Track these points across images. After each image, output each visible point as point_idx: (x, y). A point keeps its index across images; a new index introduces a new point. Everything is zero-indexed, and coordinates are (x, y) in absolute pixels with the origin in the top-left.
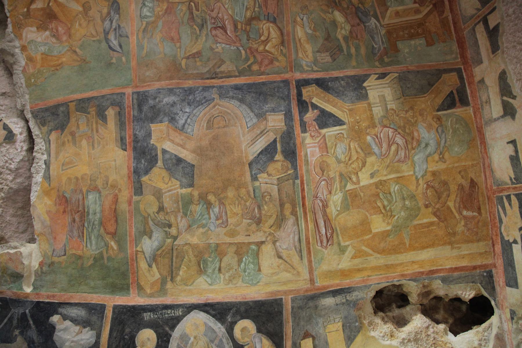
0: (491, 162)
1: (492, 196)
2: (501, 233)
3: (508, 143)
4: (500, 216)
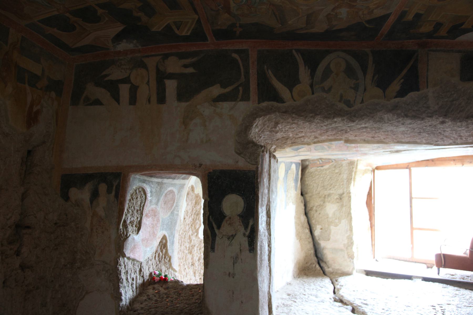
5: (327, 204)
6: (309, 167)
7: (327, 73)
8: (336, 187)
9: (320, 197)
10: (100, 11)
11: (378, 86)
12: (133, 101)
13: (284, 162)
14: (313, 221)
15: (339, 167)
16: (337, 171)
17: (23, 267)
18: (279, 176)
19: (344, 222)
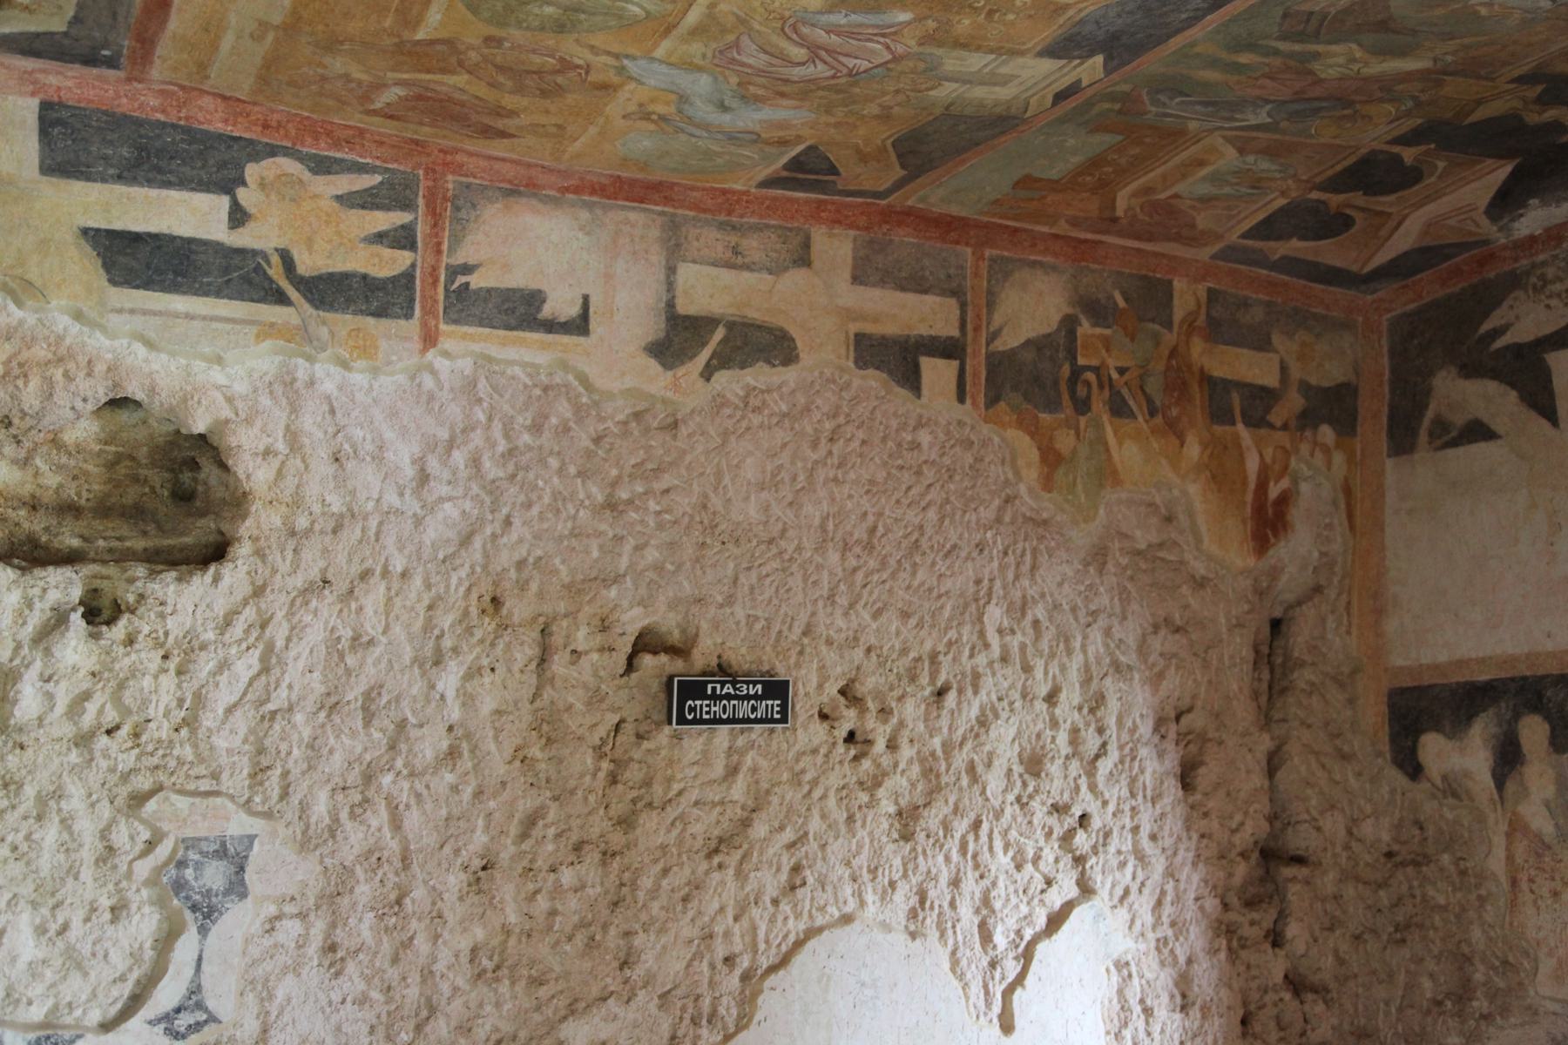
0: (547, 200)
1: (424, 159)
2: (273, 151)
3: (586, 299)
4: (342, 171)
10: (1408, 155)
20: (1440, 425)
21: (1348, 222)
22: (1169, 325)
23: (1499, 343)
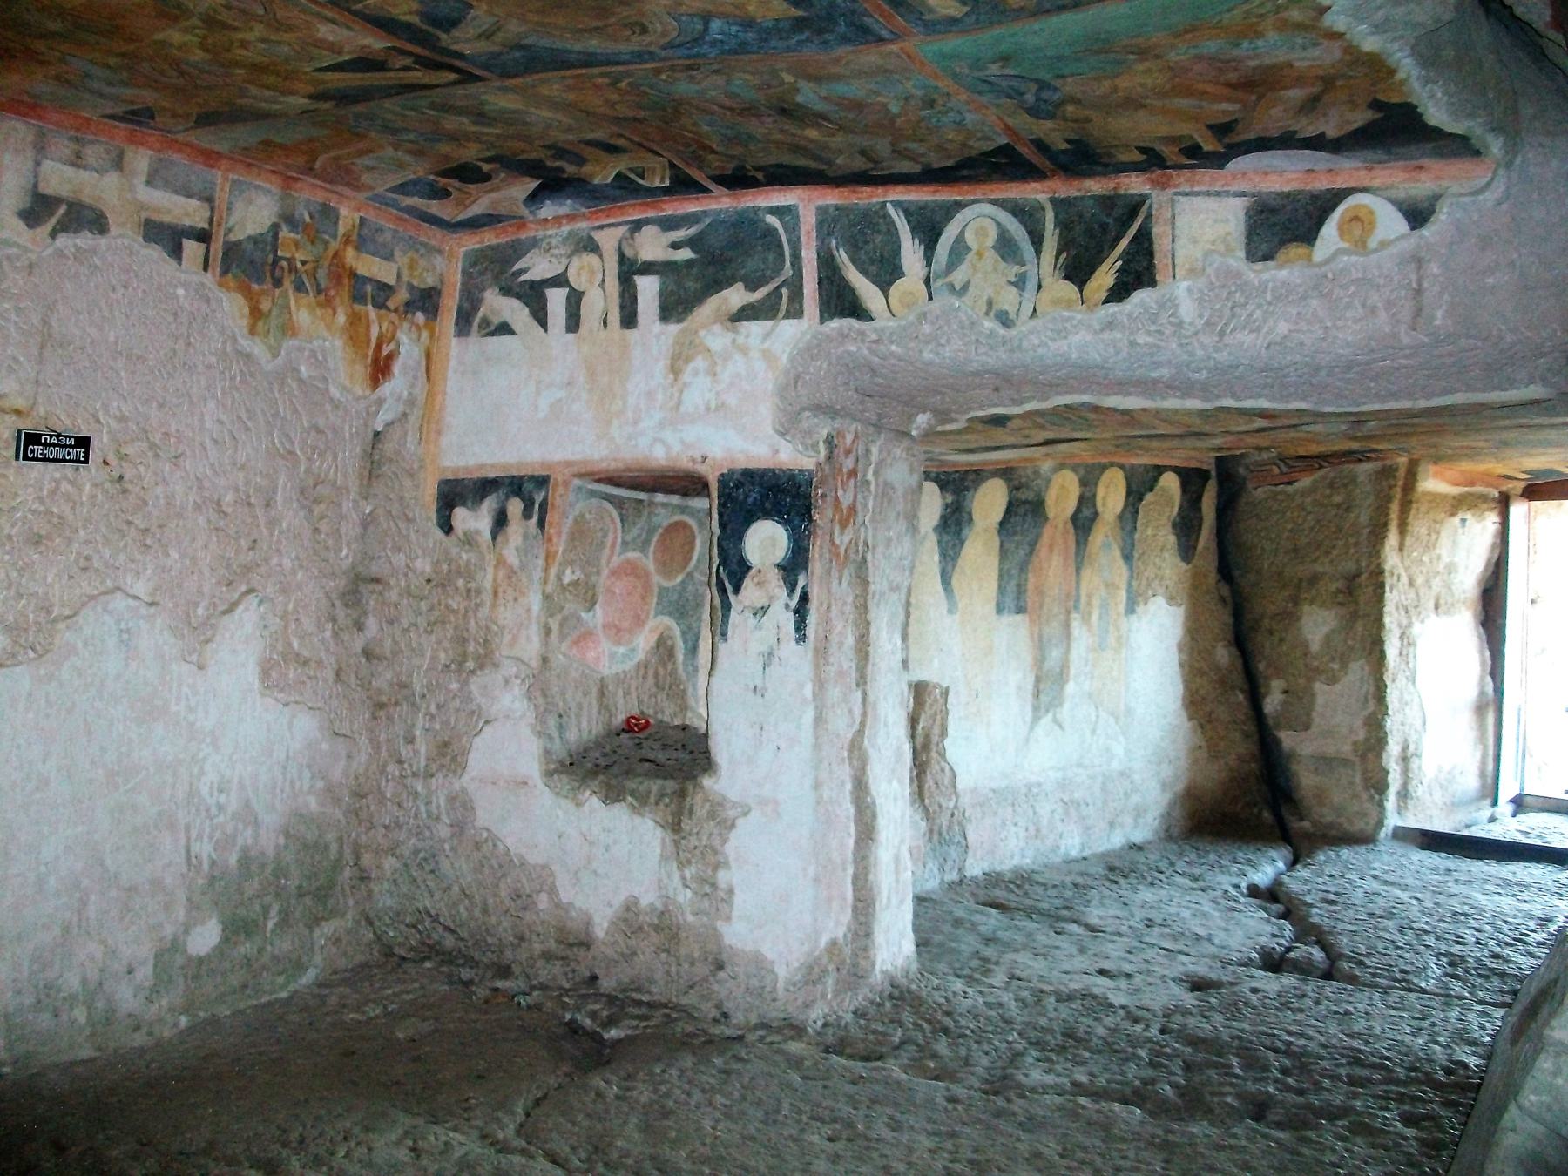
5: (1306, 608)
6: (1250, 486)
7: (959, 250)
8: (1335, 553)
9: (1284, 587)
10: (486, 167)
11: (1067, 278)
12: (573, 324)
13: (1122, 467)
14: (1261, 666)
15: (1345, 486)
16: (1337, 499)
17: (368, 654)
18: (1100, 509)
19: (1358, 669)
20: (485, 322)
21: (448, 194)
22: (335, 237)
23: (522, 278)
